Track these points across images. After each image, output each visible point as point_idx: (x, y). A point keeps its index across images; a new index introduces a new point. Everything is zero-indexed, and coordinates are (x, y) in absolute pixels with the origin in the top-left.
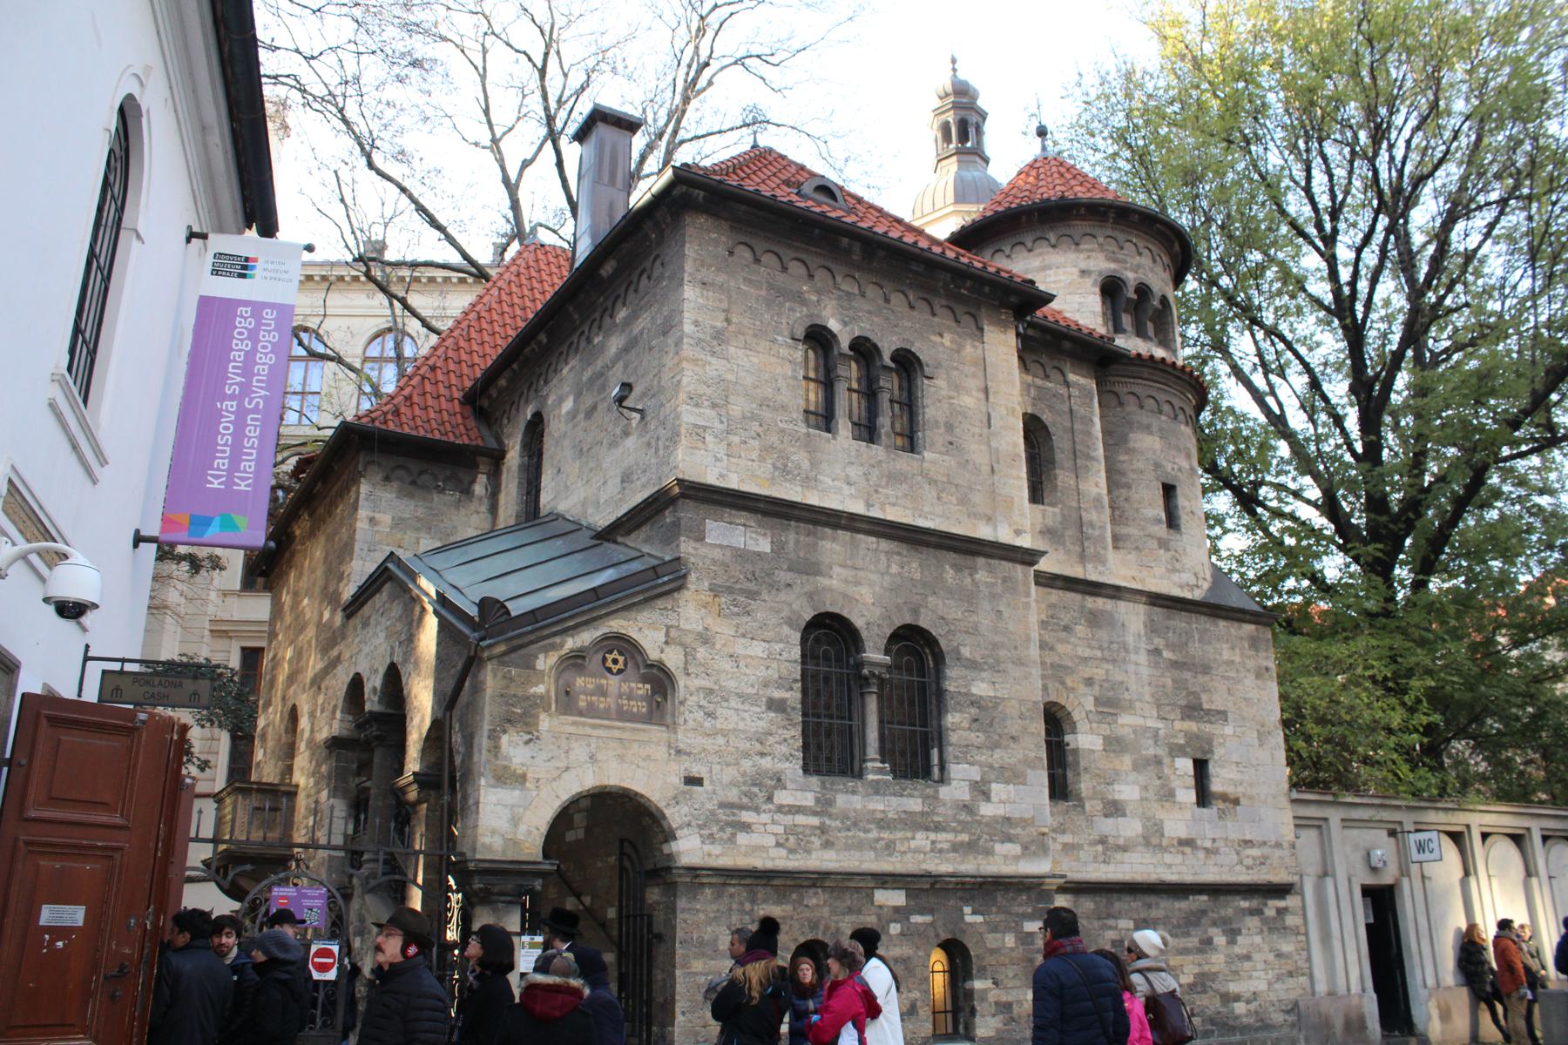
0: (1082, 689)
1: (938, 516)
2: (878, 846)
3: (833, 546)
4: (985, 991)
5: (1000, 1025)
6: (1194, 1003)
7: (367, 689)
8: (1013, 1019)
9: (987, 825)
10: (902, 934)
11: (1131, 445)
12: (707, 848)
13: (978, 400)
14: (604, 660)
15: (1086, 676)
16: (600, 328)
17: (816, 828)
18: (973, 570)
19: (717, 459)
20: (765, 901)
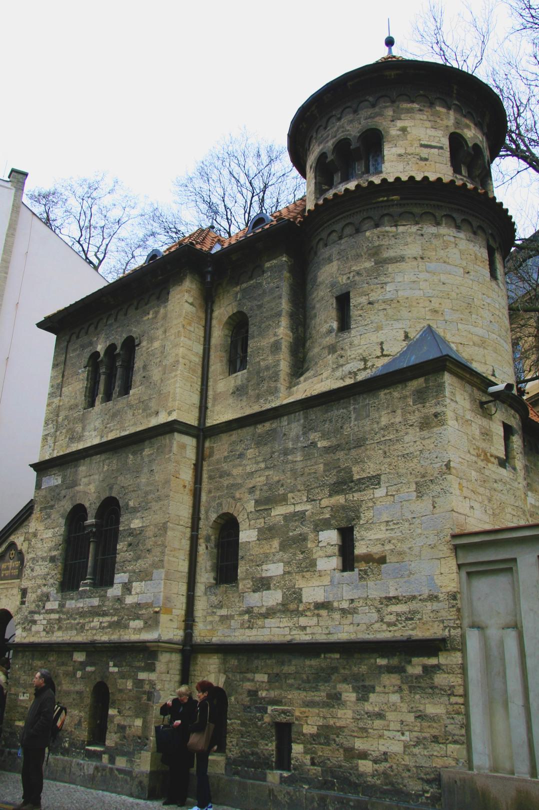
0: (247, 496)
1: (133, 425)
2: (78, 627)
4: (113, 716)
5: (118, 740)
6: (315, 753)
8: (124, 737)
9: (127, 609)
15: (251, 486)
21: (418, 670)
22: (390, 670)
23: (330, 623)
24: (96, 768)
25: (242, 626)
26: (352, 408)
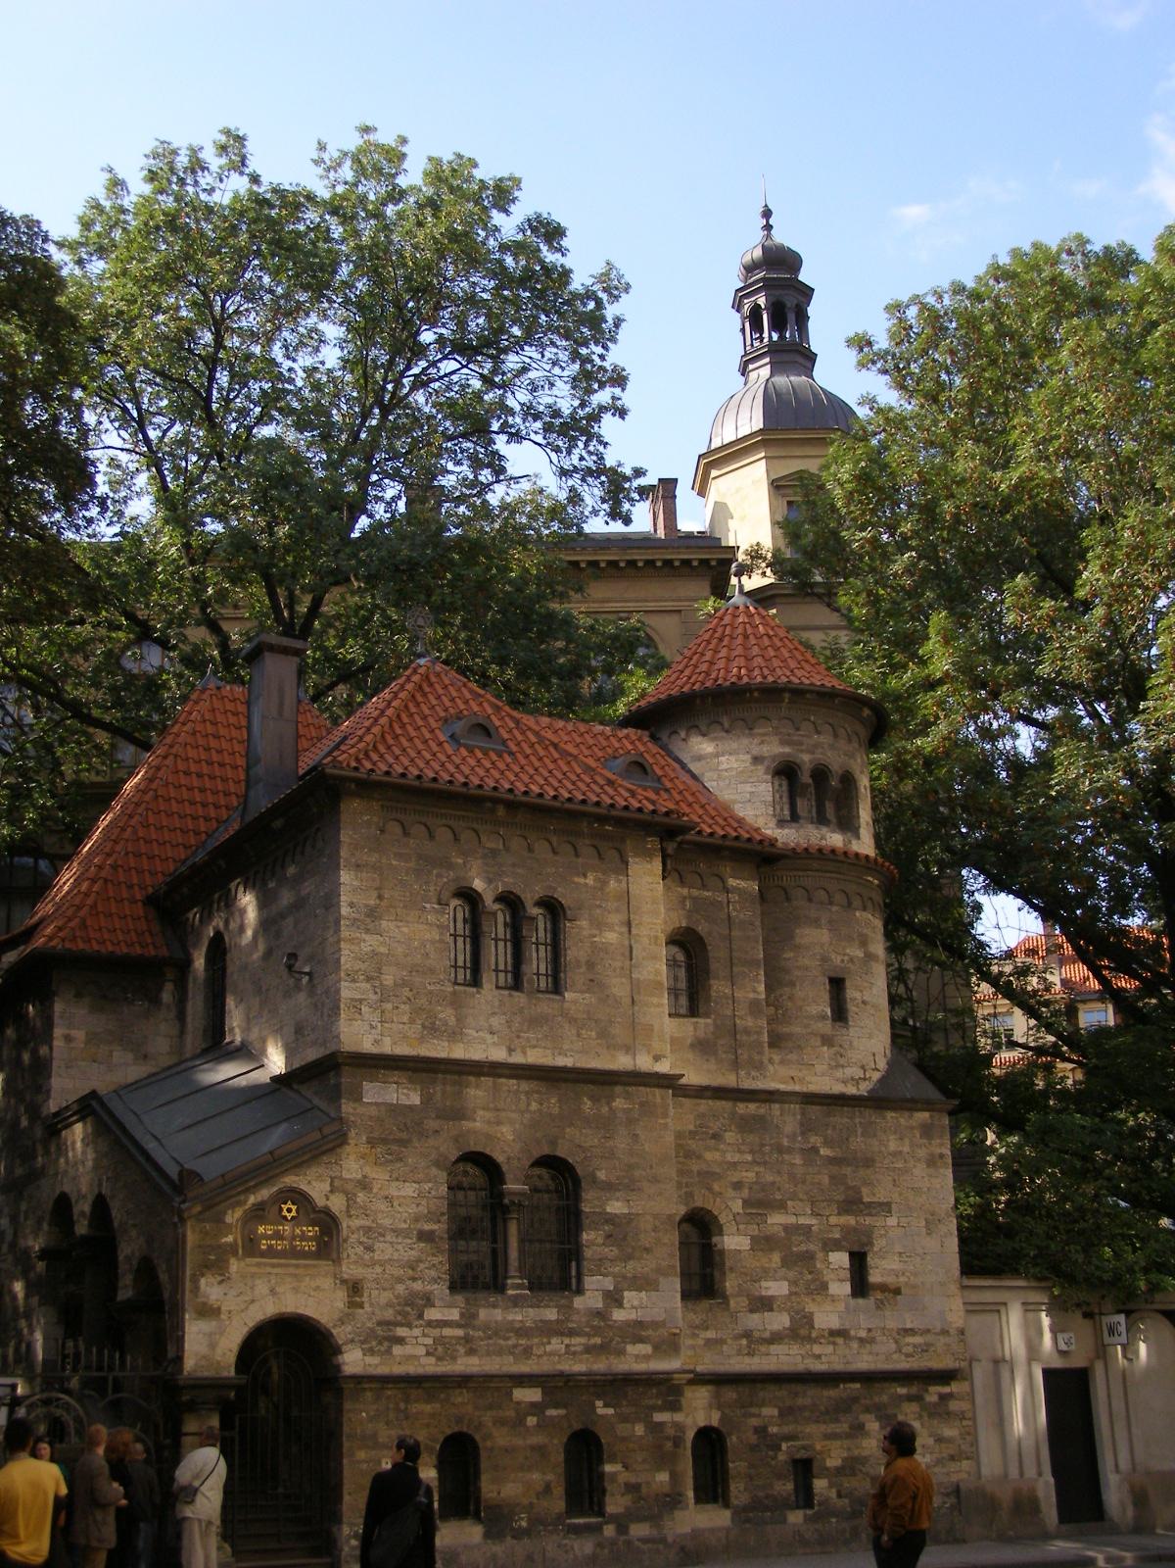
0: (731, 1193)
3: (477, 1093)
4: (614, 1475)
7: (76, 1210)
8: (641, 1498)
10: (538, 1425)
11: (798, 941)
12: (369, 1360)
13: (621, 934)
14: (281, 1210)
16: (273, 874)
17: (459, 1338)
18: (611, 1098)
19: (372, 1027)
20: (416, 1401)
21: (934, 1399)
22: (910, 1398)
23: (847, 1351)
24: (600, 1545)
25: (739, 1353)
26: (857, 1120)
